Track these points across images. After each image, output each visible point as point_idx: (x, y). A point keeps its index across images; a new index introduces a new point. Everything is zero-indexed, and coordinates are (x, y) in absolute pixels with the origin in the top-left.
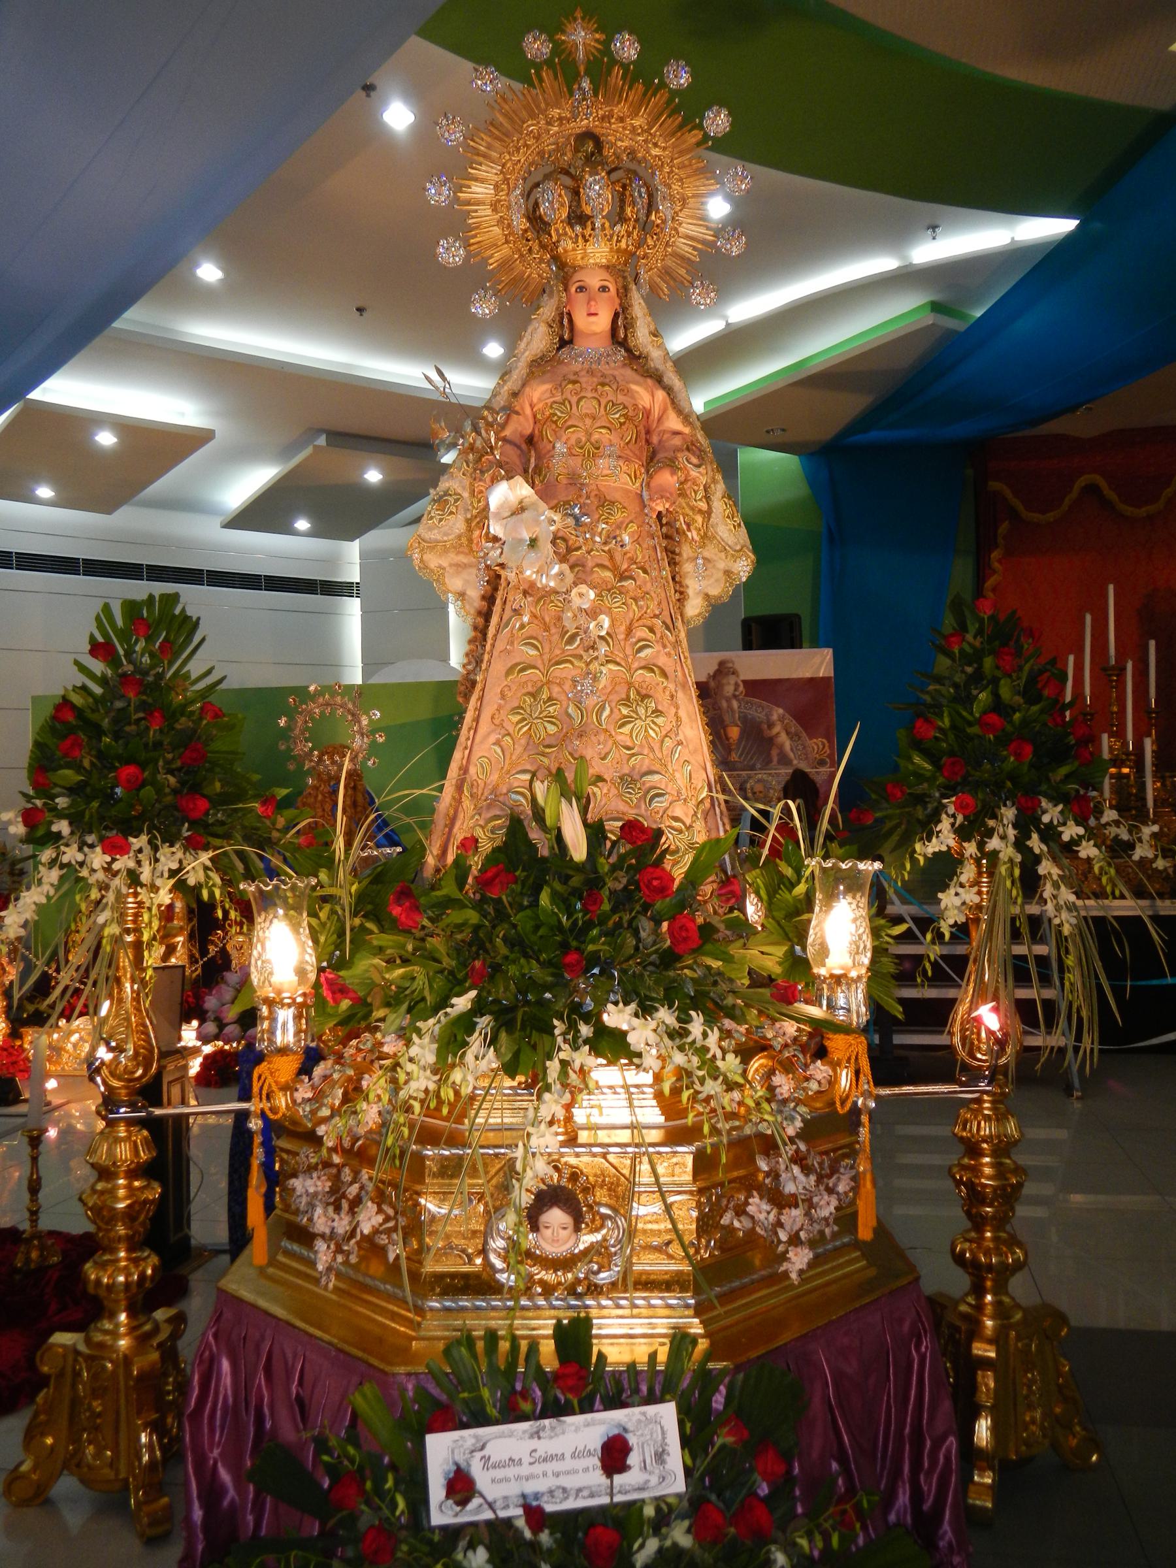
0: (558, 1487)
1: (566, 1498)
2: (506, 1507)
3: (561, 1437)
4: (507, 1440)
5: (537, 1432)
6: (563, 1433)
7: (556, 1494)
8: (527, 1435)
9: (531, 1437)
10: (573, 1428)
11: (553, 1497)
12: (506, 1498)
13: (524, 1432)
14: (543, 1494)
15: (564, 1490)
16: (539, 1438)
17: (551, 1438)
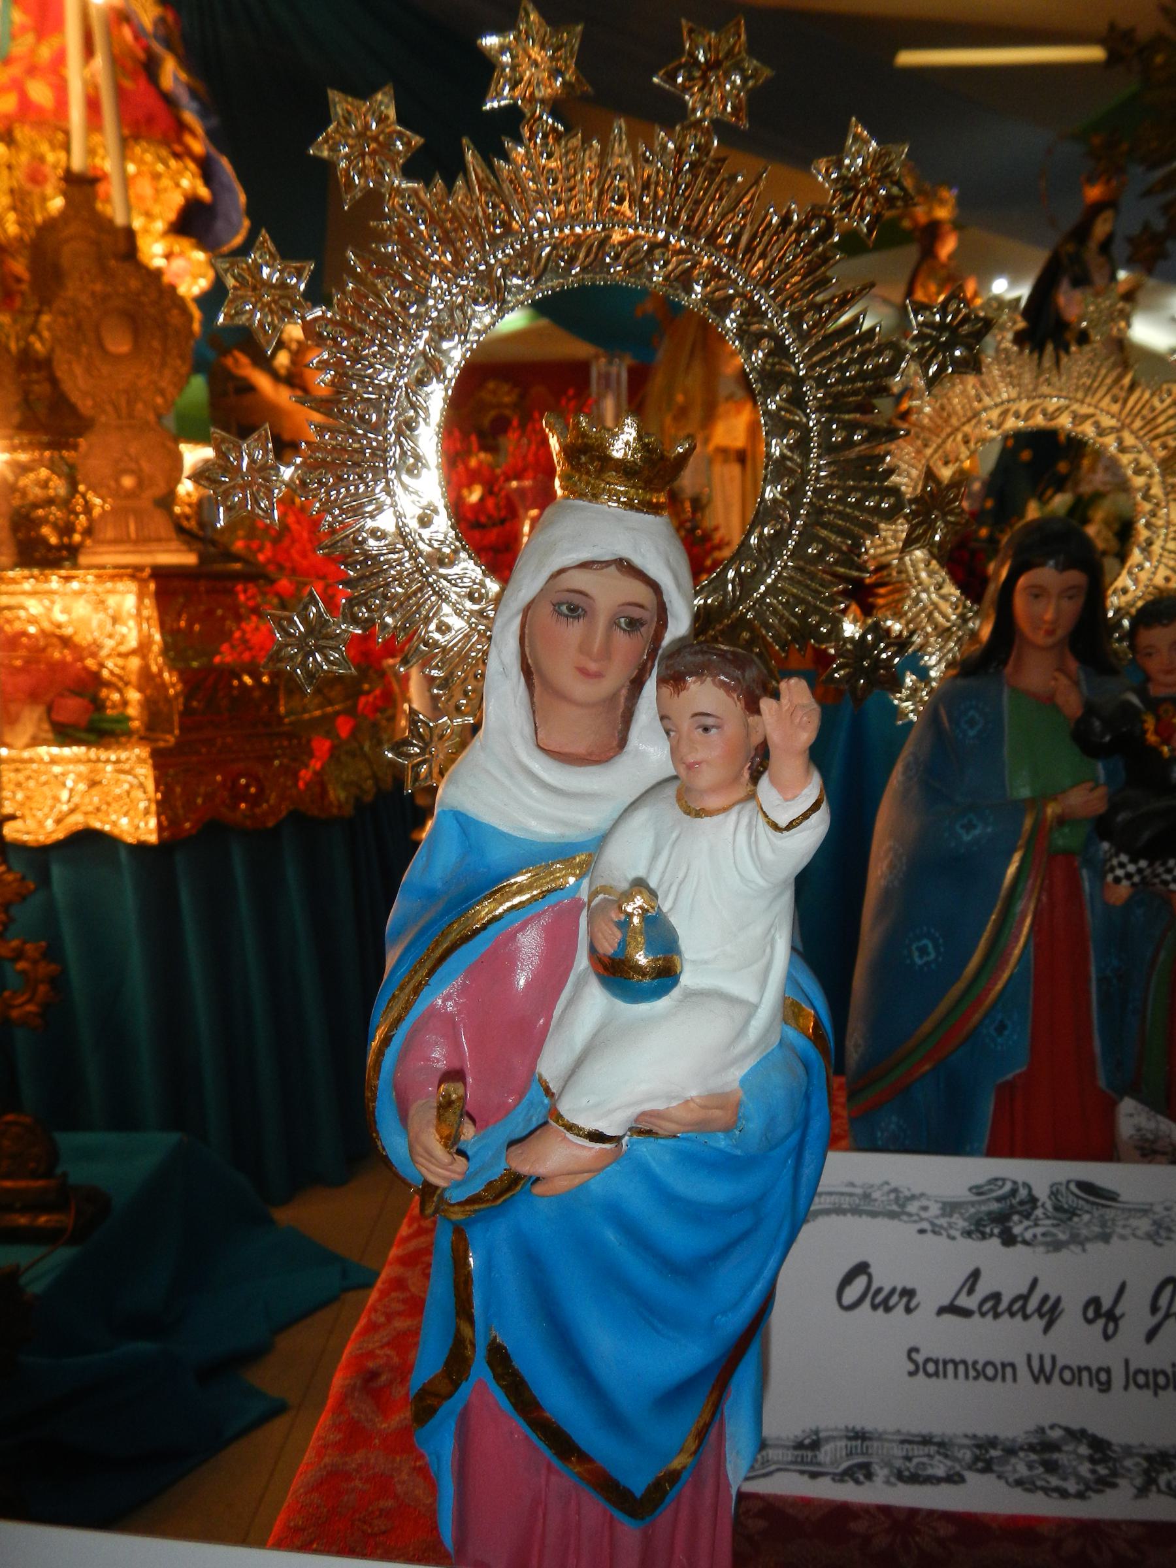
0: (1076, 1435)
1: (1105, 1483)
2: (861, 1472)
3: (1096, 1249)
4: (882, 1222)
5: (1001, 1219)
6: (1105, 1238)
7: (1060, 1457)
8: (962, 1224)
9: (977, 1229)
10: (1144, 1225)
11: (1051, 1467)
12: (860, 1436)
13: (950, 1208)
14: (1011, 1451)
15: (1099, 1447)
16: (1009, 1240)
17: (1056, 1246)
